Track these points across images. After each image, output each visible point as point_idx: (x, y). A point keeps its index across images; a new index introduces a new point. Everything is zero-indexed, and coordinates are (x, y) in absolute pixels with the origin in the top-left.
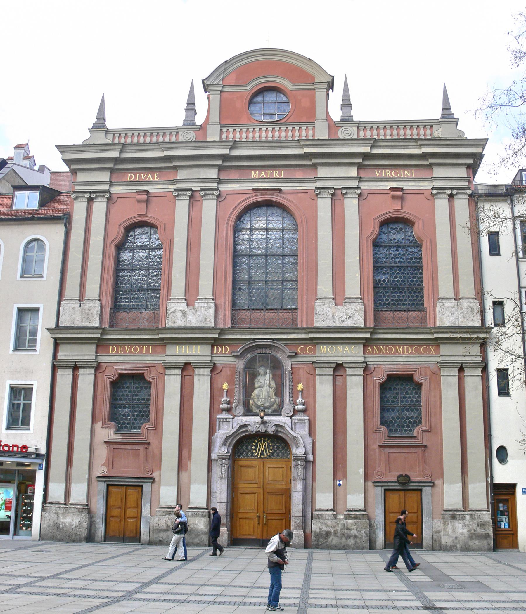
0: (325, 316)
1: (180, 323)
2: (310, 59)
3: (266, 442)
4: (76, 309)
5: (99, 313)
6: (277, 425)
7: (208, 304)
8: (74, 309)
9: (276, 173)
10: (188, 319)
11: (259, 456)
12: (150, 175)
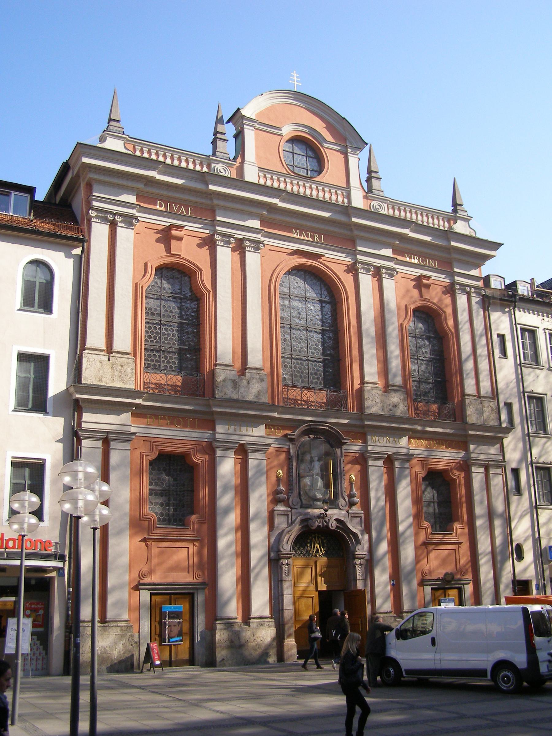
2: (344, 118)
3: (320, 539)
4: (104, 363)
5: (134, 371)
6: (337, 520)
8: (101, 362)
9: (316, 236)
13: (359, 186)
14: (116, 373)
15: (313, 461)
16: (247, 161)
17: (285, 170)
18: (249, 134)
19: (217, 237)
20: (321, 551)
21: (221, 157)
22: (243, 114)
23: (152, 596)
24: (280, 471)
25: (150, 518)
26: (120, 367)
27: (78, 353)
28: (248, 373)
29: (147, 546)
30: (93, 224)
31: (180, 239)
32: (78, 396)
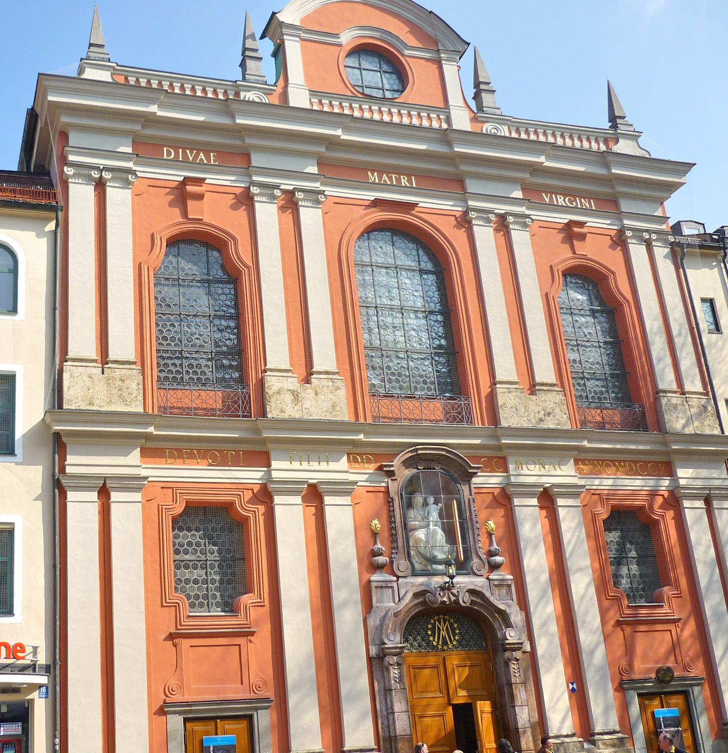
0: (514, 410)
1: (292, 412)
3: (447, 622)
5: (141, 386)
7: (333, 382)
10: (305, 406)
11: (440, 647)
12: (201, 154)
13: (462, 104)
14: (115, 391)
15: (428, 505)
16: (292, 84)
17: (349, 92)
18: (293, 49)
19: (254, 190)
20: (451, 641)
21: (253, 81)
22: (281, 19)
23: (188, 725)
24: (376, 522)
25: (176, 603)
26: (120, 383)
27: (57, 367)
28: (314, 379)
29: (175, 645)
30: (71, 185)
31: (200, 197)
32: (57, 428)
